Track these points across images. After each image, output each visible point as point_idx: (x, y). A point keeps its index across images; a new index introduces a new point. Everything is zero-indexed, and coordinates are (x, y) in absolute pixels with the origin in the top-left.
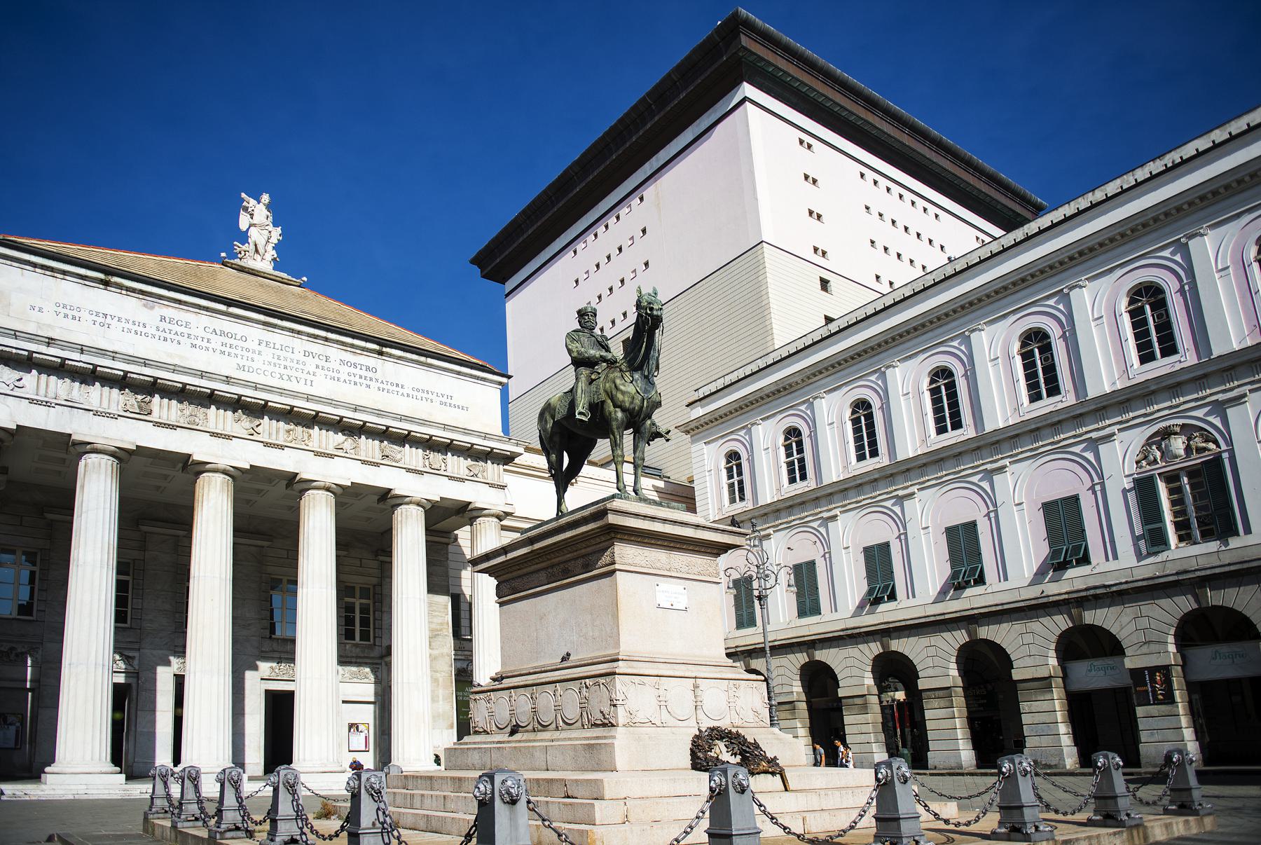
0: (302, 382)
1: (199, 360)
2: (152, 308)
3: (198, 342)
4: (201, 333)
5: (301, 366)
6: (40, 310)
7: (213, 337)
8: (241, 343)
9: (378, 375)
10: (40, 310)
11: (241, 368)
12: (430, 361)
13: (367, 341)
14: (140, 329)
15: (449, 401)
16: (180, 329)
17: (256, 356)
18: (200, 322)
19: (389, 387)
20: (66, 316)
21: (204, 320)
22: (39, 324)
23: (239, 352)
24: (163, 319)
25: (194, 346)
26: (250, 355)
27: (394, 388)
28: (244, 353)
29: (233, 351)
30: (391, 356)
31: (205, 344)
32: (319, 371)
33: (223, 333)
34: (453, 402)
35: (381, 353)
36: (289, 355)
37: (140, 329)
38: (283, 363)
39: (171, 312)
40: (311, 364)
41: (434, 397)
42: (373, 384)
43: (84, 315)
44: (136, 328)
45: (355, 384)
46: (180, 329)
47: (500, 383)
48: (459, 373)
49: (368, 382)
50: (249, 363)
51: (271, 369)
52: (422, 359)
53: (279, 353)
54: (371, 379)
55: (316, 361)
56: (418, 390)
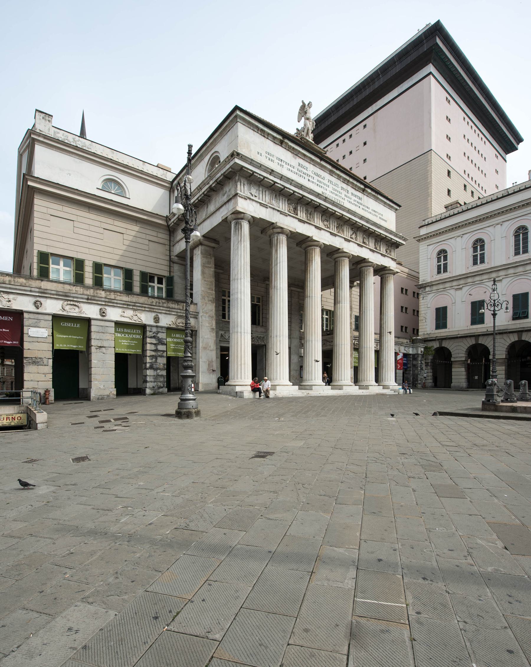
2: (296, 158)
4: (310, 173)
14: (292, 169)
16: (305, 171)
17: (327, 188)
18: (311, 169)
25: (309, 180)
29: (320, 184)
30: (367, 191)
32: (345, 197)
33: (318, 175)
35: (364, 190)
44: (291, 168)
46: (305, 171)
52: (376, 195)
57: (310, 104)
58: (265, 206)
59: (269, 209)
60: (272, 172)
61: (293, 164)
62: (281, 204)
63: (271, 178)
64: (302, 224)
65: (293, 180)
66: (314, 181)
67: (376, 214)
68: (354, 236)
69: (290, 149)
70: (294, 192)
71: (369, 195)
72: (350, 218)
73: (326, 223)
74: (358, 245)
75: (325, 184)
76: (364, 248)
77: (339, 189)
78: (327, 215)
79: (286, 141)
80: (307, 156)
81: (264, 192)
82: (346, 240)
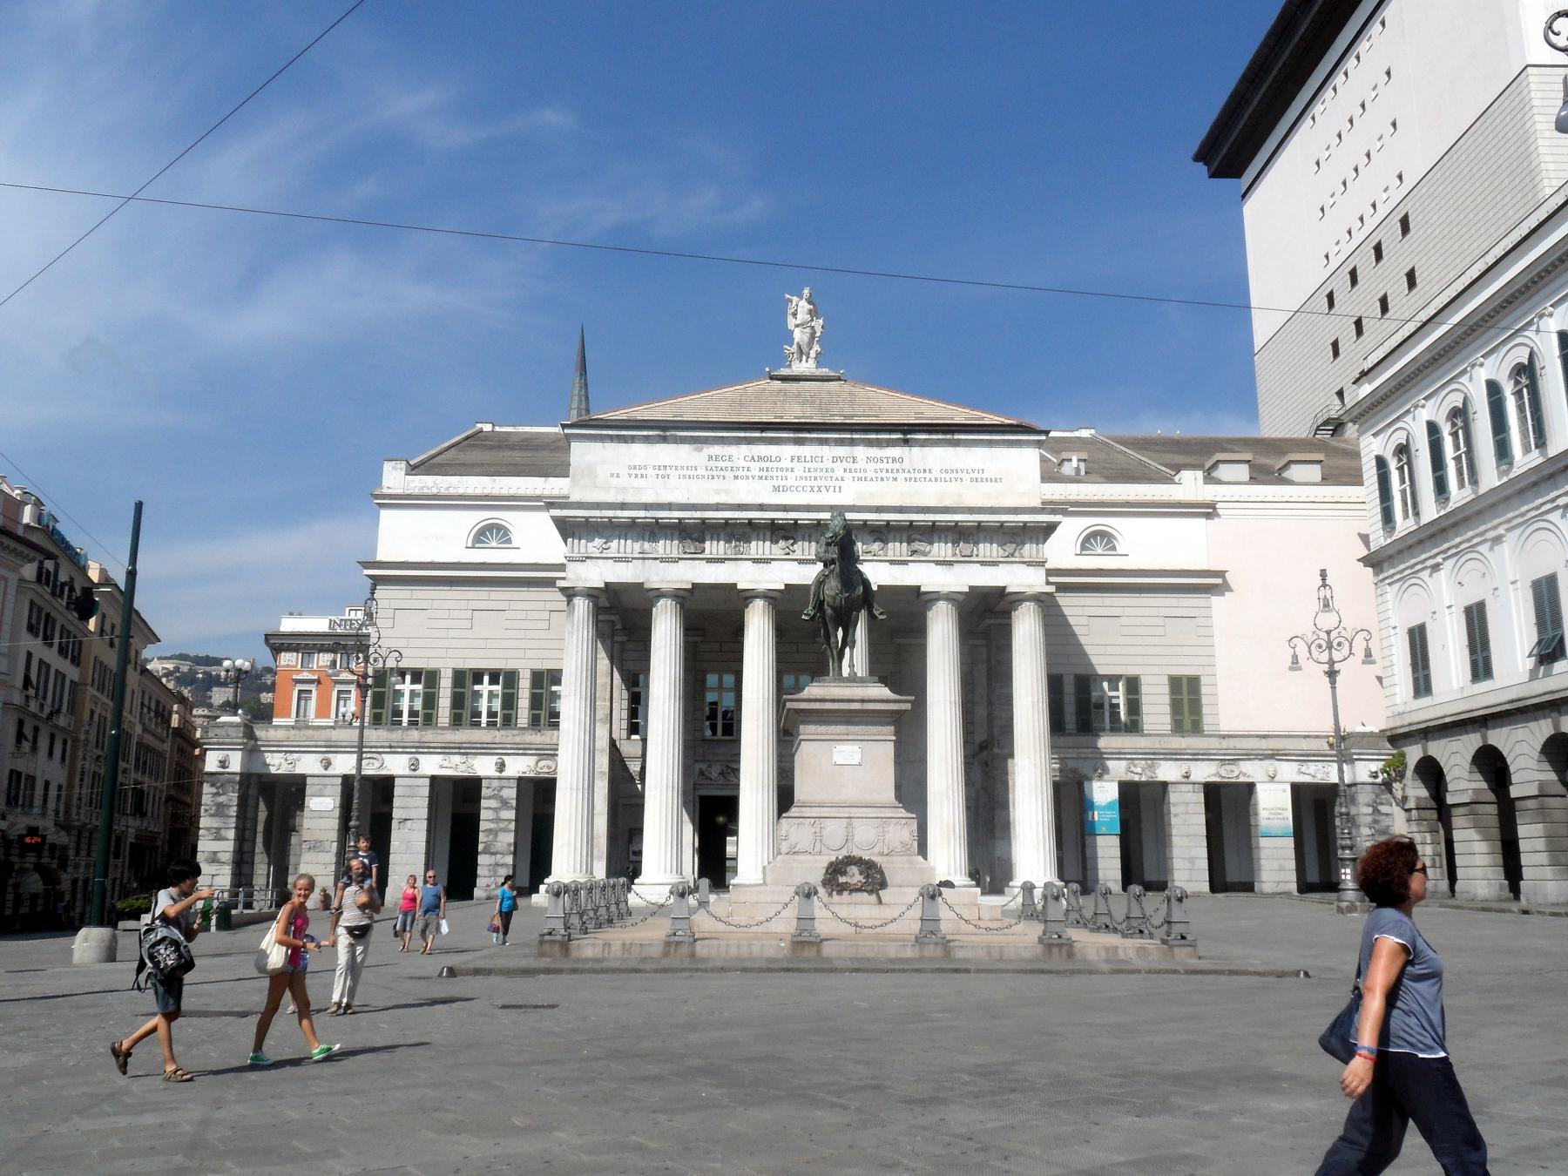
3: (739, 473)
4: (742, 463)
7: (753, 465)
9: (906, 465)
11: (776, 489)
13: (891, 432)
14: (693, 473)
16: (724, 464)
17: (789, 474)
18: (741, 453)
19: (917, 475)
22: (618, 490)
24: (710, 458)
25: (736, 477)
31: (746, 473)
32: (847, 475)
35: (906, 442)
36: (820, 465)
37: (693, 473)
39: (717, 450)
40: (839, 466)
41: (964, 476)
42: (901, 476)
43: (650, 472)
46: (724, 464)
51: (803, 483)
58: (626, 560)
60: (623, 506)
61: (692, 463)
67: (960, 475)
69: (683, 440)
71: (924, 443)
73: (782, 543)
74: (892, 562)
77: (828, 464)
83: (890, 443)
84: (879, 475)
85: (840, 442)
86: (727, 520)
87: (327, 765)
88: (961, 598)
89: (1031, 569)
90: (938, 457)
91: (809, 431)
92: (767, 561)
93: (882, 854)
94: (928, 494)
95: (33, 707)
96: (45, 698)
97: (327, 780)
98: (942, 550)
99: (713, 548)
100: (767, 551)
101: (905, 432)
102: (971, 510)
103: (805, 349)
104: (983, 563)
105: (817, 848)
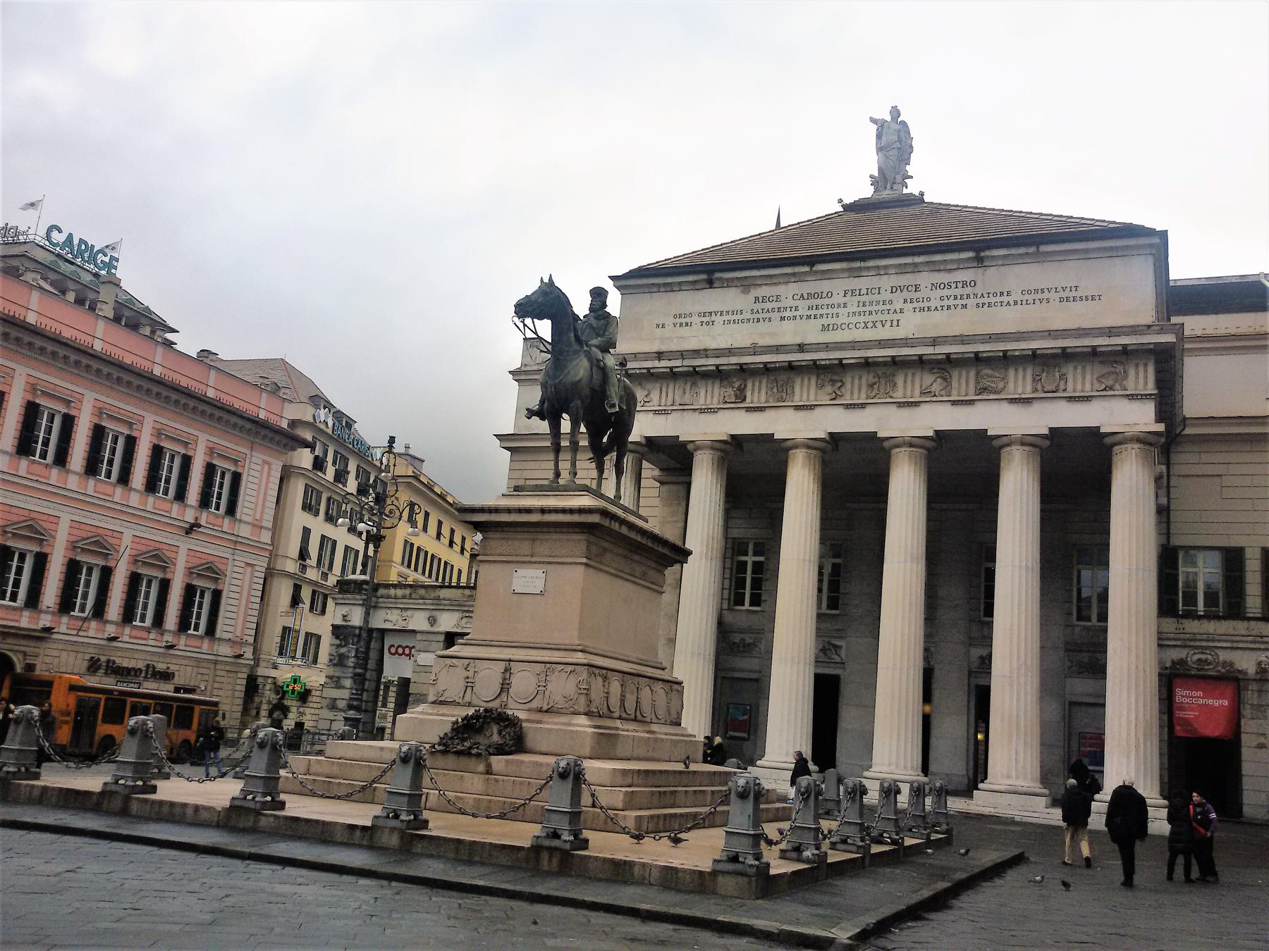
0: (889, 323)
1: (788, 333)
3: (787, 314)
4: (790, 302)
5: (888, 307)
6: (663, 326)
7: (800, 303)
8: (826, 301)
9: (978, 290)
10: (663, 326)
11: (825, 328)
12: (1044, 248)
13: (960, 250)
14: (739, 317)
15: (1074, 293)
16: (769, 305)
17: (841, 311)
19: (992, 300)
20: (681, 325)
21: (794, 288)
22: (662, 340)
23: (824, 311)
26: (835, 311)
27: (999, 299)
28: (830, 311)
29: (820, 311)
32: (909, 306)
33: (811, 296)
34: (1078, 294)
36: (876, 297)
37: (739, 317)
38: (868, 308)
41: (1053, 295)
42: (971, 302)
43: (696, 320)
45: (949, 307)
46: (769, 305)
47: (1151, 246)
48: (1086, 251)
49: (964, 302)
50: (830, 321)
51: (854, 320)
52: (1032, 249)
53: (863, 299)
54: (968, 296)
55: (905, 294)
56: (1030, 292)
57: (895, 112)
58: (665, 412)
59: (675, 414)
60: (660, 355)
62: (703, 393)
63: (664, 363)
64: (757, 414)
65: (706, 350)
66: (797, 313)
68: (936, 388)
69: (729, 284)
70: (717, 366)
72: (893, 357)
73: (829, 389)
74: (954, 403)
75: (833, 306)
76: (979, 406)
78: (830, 372)
79: (718, 275)
80: (775, 276)
81: (664, 389)
82: (901, 405)
83: (960, 266)
84: (946, 303)
85: (902, 270)
86: (765, 364)
87: (432, 621)
88: (1047, 443)
89: (1136, 406)
90: (1019, 276)
91: (863, 259)
92: (811, 407)
93: (540, 711)
94: (1006, 319)
95: (312, 574)
96: (330, 568)
97: (431, 637)
98: (1019, 381)
99: (757, 393)
100: (812, 397)
101: (978, 250)
102: (1051, 334)
103: (890, 175)
104: (1071, 399)
105: (467, 698)
